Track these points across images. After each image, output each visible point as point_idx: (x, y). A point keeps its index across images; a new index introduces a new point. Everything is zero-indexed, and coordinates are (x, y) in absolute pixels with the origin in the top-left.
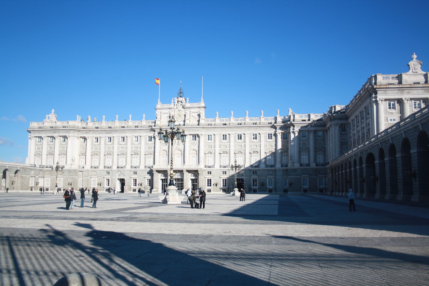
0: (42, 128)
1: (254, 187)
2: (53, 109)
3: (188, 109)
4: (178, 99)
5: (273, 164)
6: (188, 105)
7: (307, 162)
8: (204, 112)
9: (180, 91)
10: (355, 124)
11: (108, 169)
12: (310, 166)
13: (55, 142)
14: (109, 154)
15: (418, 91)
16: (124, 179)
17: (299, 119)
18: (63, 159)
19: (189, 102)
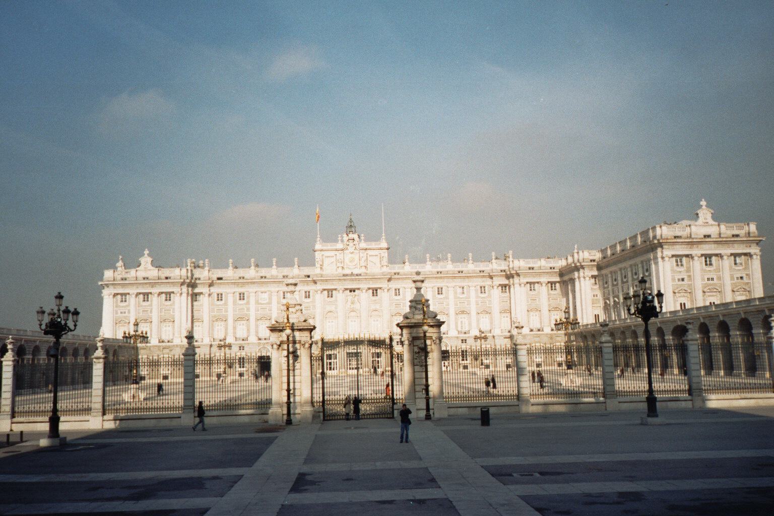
0: (128, 279)
1: (463, 362)
2: (146, 249)
3: (364, 251)
4: (348, 236)
5: (489, 329)
6: (363, 245)
7: (539, 326)
8: (386, 255)
9: (349, 224)
10: (619, 278)
11: (243, 342)
12: (543, 331)
13: (152, 301)
14: (240, 319)
15: (710, 245)
16: (268, 358)
17: (525, 266)
18: (167, 328)
19: (366, 240)
